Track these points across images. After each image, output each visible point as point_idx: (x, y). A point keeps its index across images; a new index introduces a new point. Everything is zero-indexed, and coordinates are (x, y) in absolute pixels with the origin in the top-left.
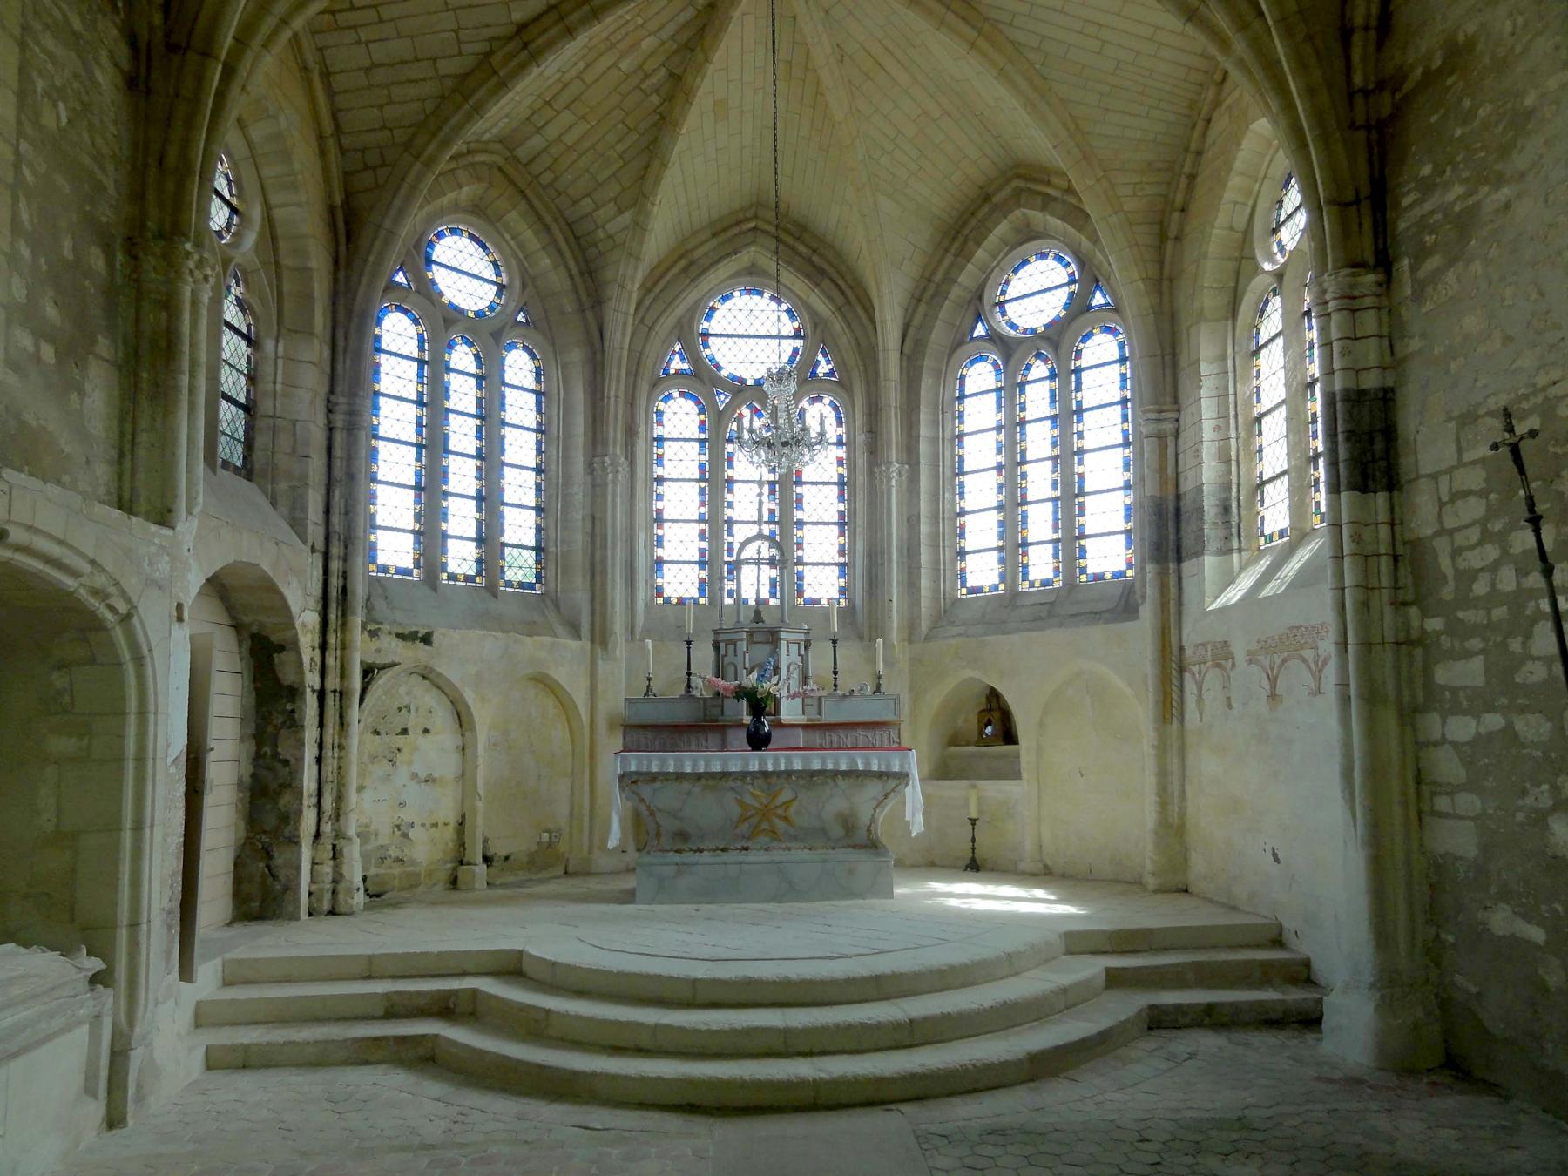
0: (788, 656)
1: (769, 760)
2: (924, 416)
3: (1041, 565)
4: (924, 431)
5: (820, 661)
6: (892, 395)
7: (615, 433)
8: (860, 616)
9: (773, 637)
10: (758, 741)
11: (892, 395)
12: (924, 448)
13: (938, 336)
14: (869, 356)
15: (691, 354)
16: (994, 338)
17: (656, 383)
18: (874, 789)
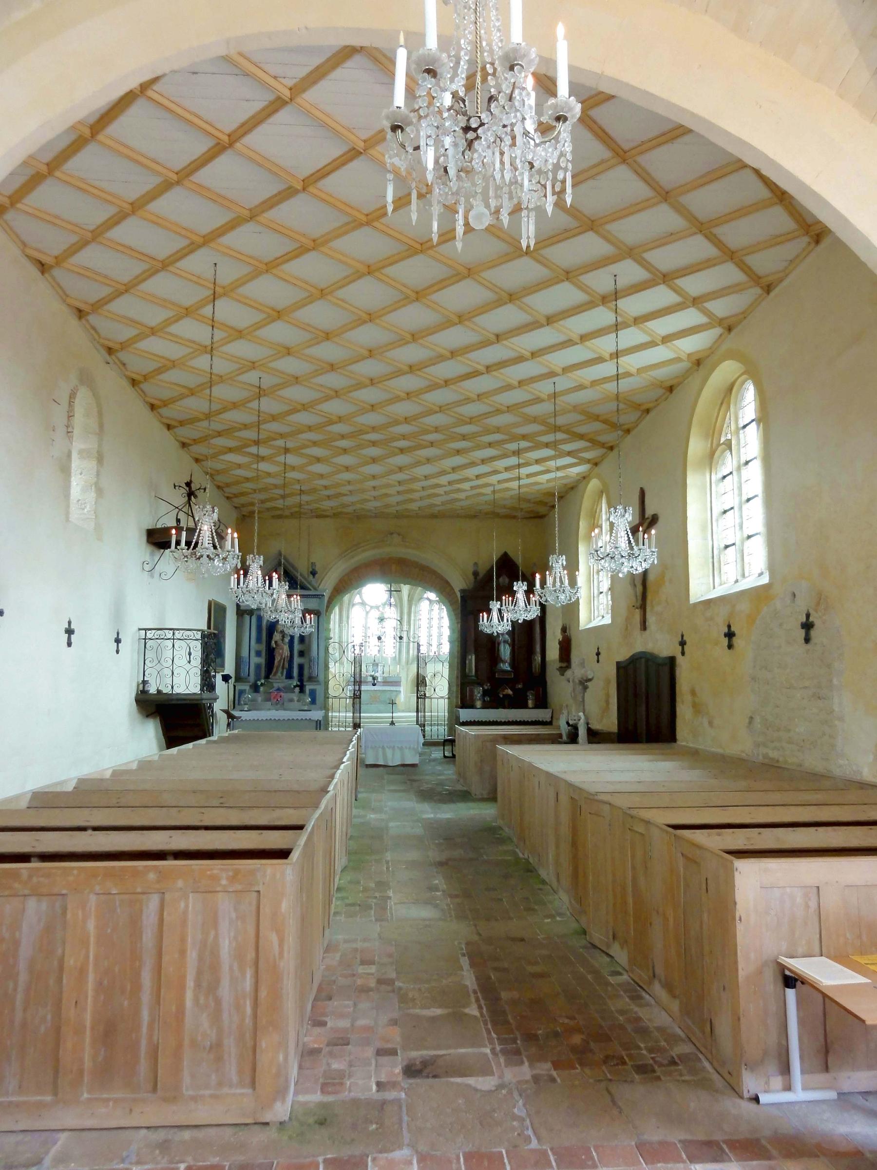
0: (380, 668)
1: (375, 688)
2: (412, 615)
3: (434, 648)
4: (412, 618)
5: (386, 669)
6: (406, 610)
7: (344, 618)
8: (397, 660)
9: (377, 665)
10: (374, 685)
11: (406, 610)
12: (412, 622)
13: (416, 597)
14: (401, 599)
15: (361, 597)
16: (428, 599)
17: (354, 605)
18: (395, 693)
